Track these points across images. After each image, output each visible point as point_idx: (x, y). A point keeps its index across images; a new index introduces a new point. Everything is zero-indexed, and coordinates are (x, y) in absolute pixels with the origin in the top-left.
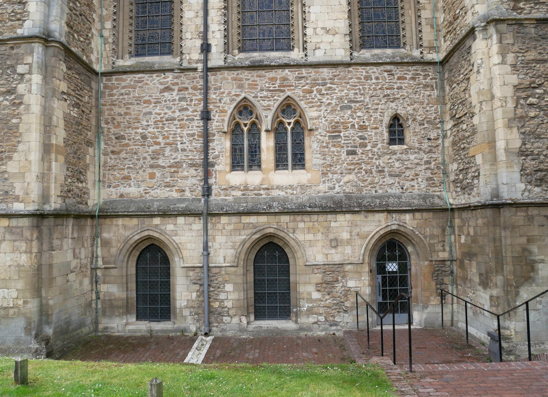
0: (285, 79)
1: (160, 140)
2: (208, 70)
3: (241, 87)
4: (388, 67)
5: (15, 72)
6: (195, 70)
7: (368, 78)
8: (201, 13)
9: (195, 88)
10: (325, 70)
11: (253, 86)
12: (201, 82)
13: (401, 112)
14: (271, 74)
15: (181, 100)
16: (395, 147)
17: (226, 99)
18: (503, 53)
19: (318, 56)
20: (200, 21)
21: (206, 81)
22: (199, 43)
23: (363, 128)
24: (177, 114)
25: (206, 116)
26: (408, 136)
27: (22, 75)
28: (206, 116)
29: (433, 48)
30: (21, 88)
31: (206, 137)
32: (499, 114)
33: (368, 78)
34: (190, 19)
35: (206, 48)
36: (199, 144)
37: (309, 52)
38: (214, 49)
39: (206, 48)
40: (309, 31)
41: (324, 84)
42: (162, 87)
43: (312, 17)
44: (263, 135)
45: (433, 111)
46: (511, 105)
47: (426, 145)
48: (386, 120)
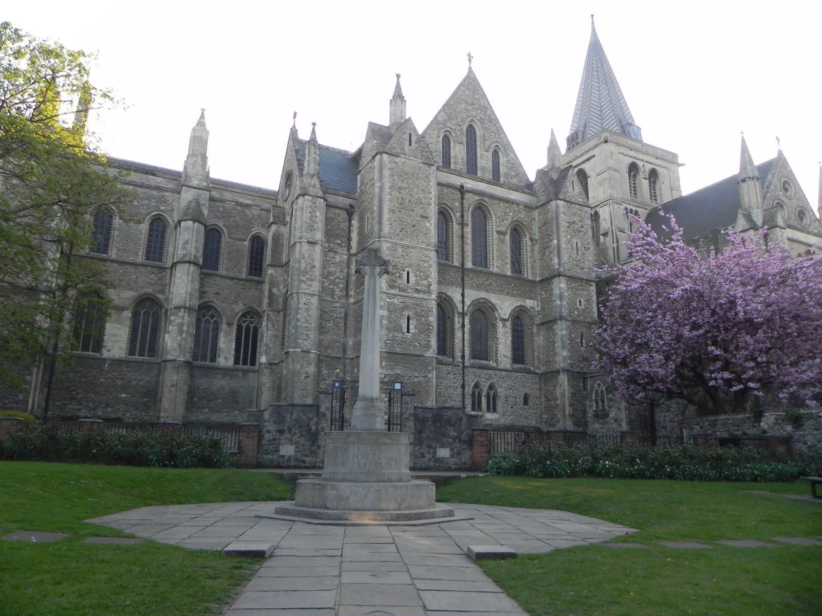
0: (490, 374)
1: (446, 395)
2: (464, 367)
3: (475, 376)
4: (524, 374)
5: (427, 368)
6: (460, 366)
7: (517, 377)
8: (461, 341)
9: (459, 374)
10: (503, 372)
11: (479, 376)
12: (461, 372)
13: (528, 392)
14: (485, 371)
15: (454, 378)
16: (525, 406)
17: (470, 380)
18: (568, 382)
19: (501, 366)
20: (461, 345)
21: (463, 372)
22: (460, 354)
23: (516, 398)
24: (452, 385)
25: (463, 387)
26: (530, 402)
27: (430, 371)
28: (463, 387)
29: (539, 368)
30: (430, 375)
31: (463, 395)
32: (567, 402)
33: (517, 377)
34: (457, 343)
35: (463, 357)
36: (460, 399)
37: (499, 364)
38: (466, 358)
39: (463, 357)
40: (499, 355)
41: (503, 378)
42: (447, 372)
43: (500, 350)
44: (483, 397)
45: (538, 393)
46: (570, 399)
47: (535, 407)
48: (523, 395)
